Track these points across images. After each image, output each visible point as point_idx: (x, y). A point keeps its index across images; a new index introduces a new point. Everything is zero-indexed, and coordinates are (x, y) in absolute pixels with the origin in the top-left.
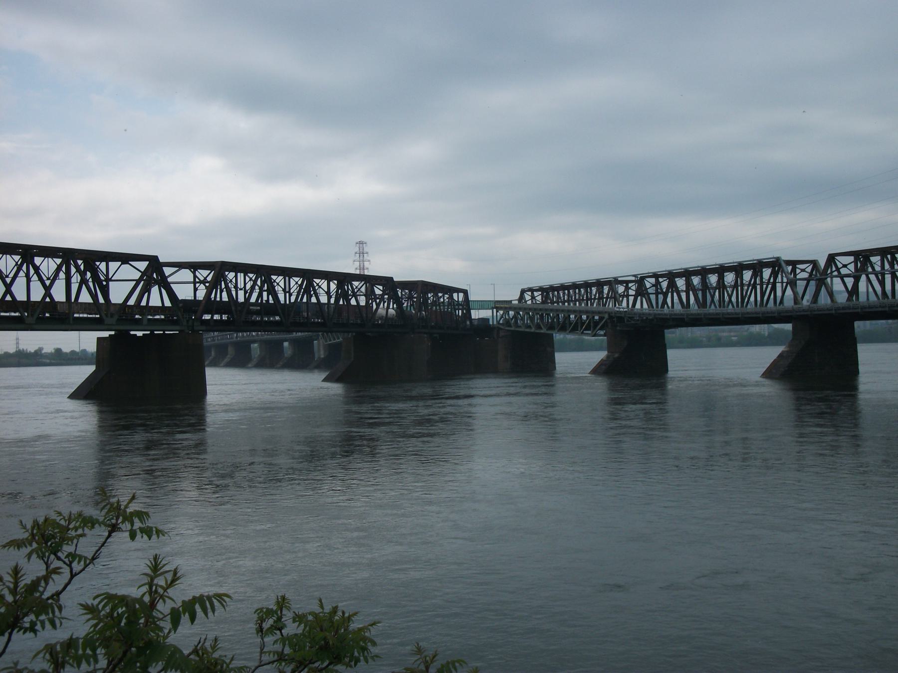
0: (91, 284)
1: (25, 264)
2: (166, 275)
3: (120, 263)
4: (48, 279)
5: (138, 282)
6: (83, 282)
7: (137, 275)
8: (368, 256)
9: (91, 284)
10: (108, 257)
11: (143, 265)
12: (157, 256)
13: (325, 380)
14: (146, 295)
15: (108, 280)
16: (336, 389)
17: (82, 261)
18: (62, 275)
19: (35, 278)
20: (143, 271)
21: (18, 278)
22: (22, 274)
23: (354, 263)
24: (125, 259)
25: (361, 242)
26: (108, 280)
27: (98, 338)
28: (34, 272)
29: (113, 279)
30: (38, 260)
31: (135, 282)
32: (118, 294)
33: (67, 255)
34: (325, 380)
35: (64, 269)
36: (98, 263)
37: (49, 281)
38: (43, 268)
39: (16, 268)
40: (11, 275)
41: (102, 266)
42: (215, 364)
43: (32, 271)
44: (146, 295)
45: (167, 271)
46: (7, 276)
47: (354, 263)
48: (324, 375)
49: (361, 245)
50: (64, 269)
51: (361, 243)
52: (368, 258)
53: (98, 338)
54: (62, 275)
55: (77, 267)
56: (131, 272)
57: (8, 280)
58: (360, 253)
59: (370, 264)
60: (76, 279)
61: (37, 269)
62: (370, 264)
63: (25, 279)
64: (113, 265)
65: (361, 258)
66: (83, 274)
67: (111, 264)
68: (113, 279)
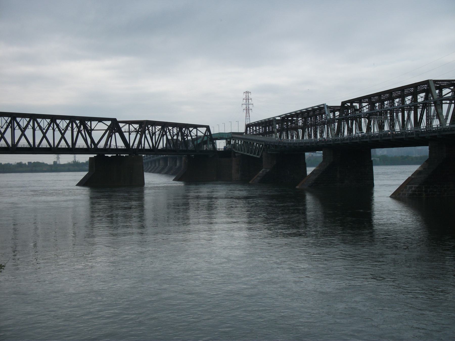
0: (83, 132)
1: (52, 123)
2: (121, 127)
3: (98, 122)
4: (63, 130)
5: (106, 131)
6: (79, 131)
7: (106, 127)
8: (252, 101)
9: (83, 132)
10: (91, 119)
11: (109, 123)
12: (116, 119)
13: (173, 180)
14: (110, 138)
15: (92, 130)
16: (180, 184)
17: (79, 121)
18: (69, 128)
19: (57, 129)
20: (109, 125)
21: (49, 130)
22: (51, 128)
23: (242, 107)
24: (100, 120)
25: (247, 92)
26: (92, 130)
27: (90, 158)
28: (56, 127)
29: (94, 129)
30: (58, 121)
31: (105, 131)
32: (96, 135)
33: (72, 119)
34: (173, 180)
35: (70, 125)
36: (86, 122)
37: (63, 131)
38: (61, 125)
39: (48, 125)
40: (46, 129)
41: (89, 123)
42: (146, 172)
43: (55, 126)
44: (110, 138)
45: (121, 125)
46: (44, 129)
47: (242, 107)
48: (173, 178)
49: (247, 94)
50: (70, 125)
51: (247, 92)
52: (252, 103)
53: (90, 158)
54: (69, 128)
55: (76, 124)
56: (103, 126)
57: (44, 131)
58: (246, 99)
59: (253, 106)
60: (76, 130)
61: (58, 126)
62: (253, 106)
63: (52, 130)
64: (94, 123)
65: (247, 102)
66: (79, 128)
67: (92, 122)
68: (94, 129)
